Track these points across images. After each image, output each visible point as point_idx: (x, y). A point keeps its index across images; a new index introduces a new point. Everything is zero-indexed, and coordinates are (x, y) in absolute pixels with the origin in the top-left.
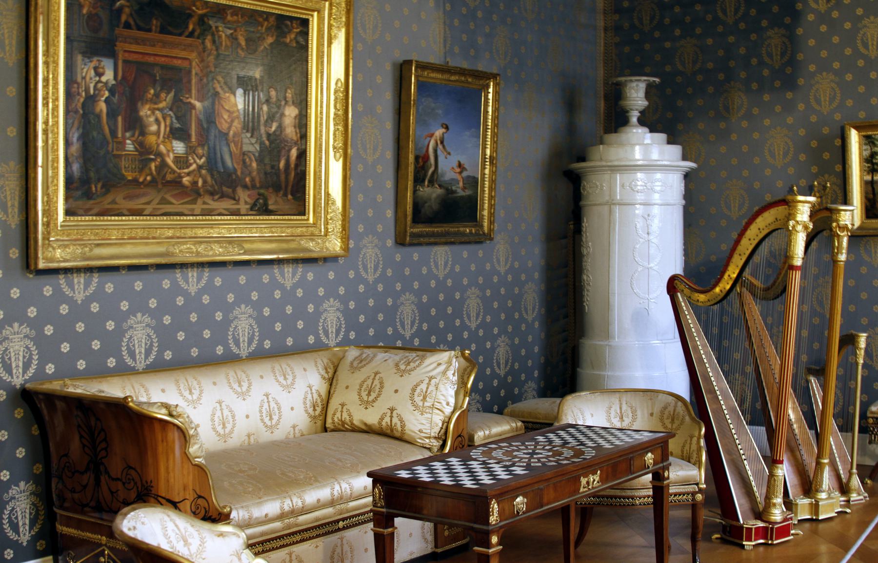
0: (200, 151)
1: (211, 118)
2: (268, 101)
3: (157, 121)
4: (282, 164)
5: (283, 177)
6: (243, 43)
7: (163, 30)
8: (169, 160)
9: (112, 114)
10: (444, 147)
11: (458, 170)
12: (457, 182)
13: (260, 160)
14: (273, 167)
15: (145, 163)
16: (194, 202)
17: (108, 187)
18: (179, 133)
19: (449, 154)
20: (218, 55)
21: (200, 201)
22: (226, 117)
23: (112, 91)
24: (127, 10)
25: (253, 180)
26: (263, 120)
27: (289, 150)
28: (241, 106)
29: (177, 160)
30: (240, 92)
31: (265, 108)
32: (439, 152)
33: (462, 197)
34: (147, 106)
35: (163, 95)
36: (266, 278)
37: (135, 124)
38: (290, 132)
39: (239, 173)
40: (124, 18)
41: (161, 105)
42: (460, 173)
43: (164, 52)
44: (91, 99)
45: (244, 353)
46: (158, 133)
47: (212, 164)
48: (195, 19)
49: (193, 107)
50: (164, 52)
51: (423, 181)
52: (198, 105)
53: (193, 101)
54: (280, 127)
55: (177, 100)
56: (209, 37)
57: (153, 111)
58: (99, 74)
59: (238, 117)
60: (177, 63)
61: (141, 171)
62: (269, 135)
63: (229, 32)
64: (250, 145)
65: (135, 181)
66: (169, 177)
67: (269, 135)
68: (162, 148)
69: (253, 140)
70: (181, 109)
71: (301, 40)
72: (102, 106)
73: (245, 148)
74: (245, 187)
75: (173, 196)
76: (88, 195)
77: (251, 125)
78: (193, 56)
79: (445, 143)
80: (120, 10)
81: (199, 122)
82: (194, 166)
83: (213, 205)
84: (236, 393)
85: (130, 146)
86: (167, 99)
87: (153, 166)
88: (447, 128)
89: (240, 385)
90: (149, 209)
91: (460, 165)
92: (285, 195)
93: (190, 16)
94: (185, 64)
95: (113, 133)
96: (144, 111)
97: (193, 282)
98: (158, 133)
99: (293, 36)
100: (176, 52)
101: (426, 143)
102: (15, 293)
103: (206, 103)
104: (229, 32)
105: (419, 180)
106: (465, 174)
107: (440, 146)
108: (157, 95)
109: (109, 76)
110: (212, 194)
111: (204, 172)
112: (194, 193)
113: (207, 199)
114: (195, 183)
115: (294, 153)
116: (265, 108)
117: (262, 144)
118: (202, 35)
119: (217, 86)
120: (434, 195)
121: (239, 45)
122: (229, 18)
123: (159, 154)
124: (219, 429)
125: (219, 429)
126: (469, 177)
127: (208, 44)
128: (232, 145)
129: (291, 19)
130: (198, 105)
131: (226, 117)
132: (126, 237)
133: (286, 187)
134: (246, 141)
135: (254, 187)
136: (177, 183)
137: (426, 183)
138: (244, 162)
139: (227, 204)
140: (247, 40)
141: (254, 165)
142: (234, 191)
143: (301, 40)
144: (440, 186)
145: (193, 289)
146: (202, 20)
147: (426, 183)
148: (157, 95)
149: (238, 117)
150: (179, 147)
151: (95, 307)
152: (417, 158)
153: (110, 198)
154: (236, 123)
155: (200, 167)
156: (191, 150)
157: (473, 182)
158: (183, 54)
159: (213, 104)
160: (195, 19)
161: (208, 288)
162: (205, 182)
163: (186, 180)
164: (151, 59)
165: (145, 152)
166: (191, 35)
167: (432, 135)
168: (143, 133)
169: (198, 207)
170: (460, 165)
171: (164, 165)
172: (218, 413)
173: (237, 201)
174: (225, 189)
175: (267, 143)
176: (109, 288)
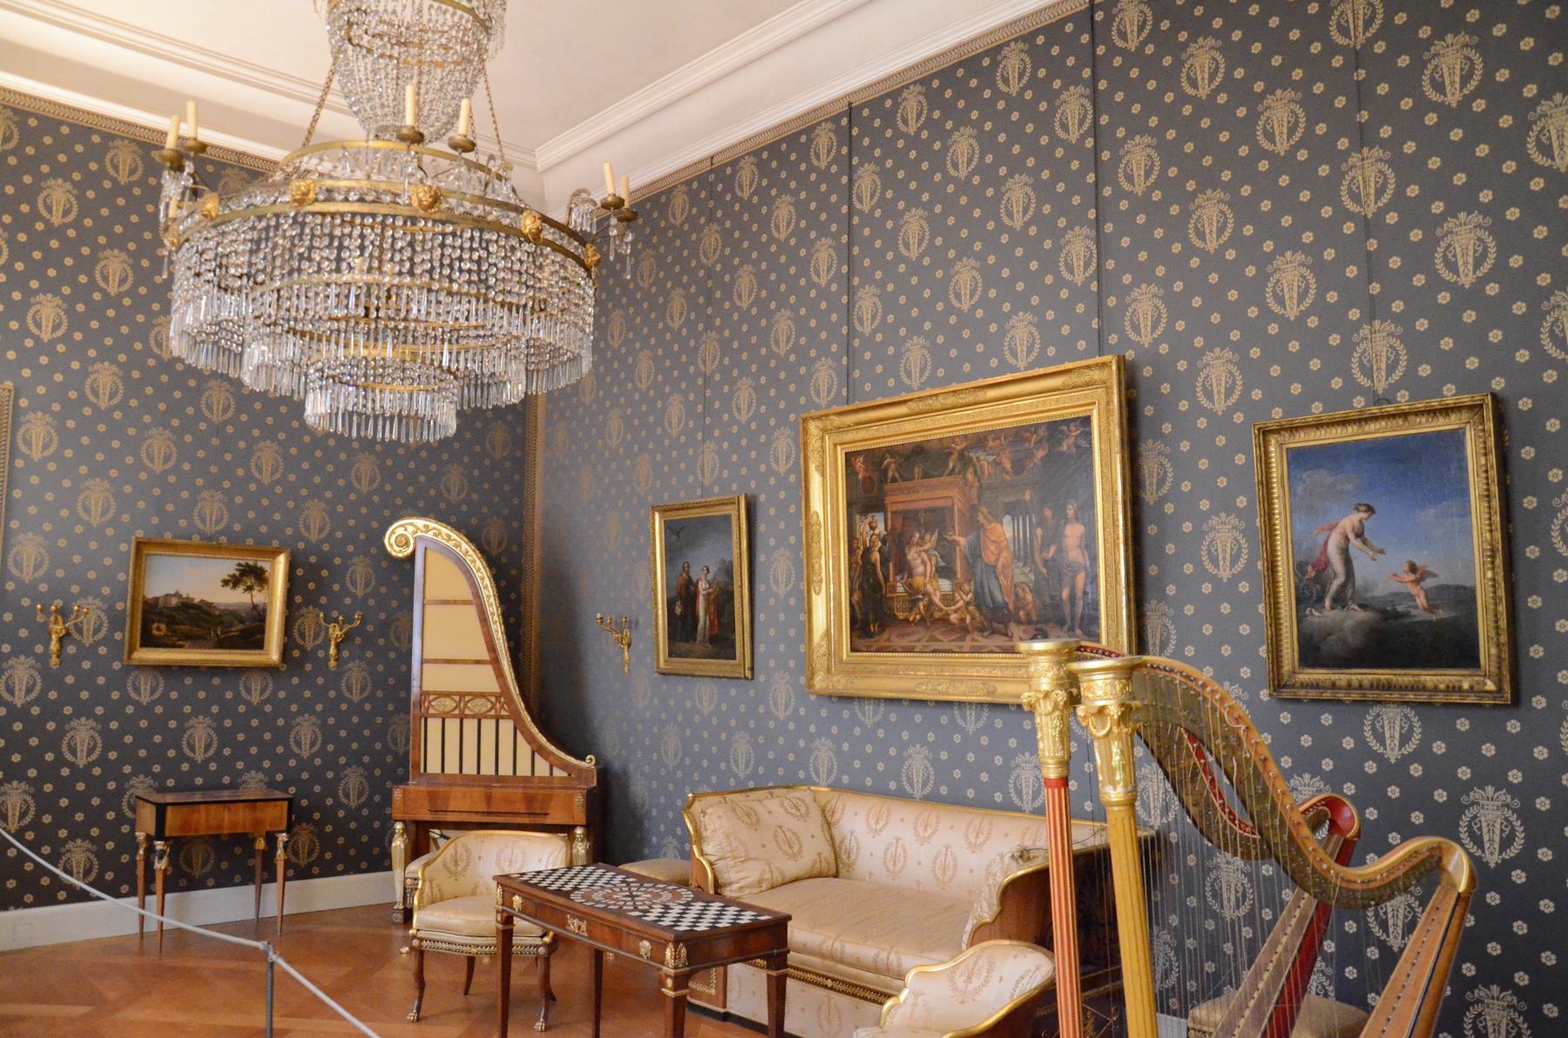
0: (966, 587)
1: (975, 553)
2: (1041, 522)
3: (923, 562)
4: (1065, 594)
5: (1067, 610)
6: (1008, 466)
7: (926, 475)
8: (937, 599)
9: (884, 562)
10: (1365, 542)
11: (1412, 577)
12: (1411, 597)
13: (1036, 591)
14: (1052, 598)
15: (914, 602)
16: (962, 639)
17: (883, 628)
18: (945, 571)
19: (1382, 552)
20: (981, 487)
21: (969, 638)
22: (992, 548)
23: (884, 541)
24: (893, 466)
25: (1028, 615)
26: (1037, 545)
27: (1074, 577)
28: (1009, 535)
29: (944, 598)
30: (1007, 519)
31: (1039, 532)
32: (1353, 552)
33: (1423, 623)
34: (913, 550)
35: (927, 537)
36: (944, 719)
37: (904, 568)
38: (1075, 554)
39: (1011, 607)
40: (890, 474)
41: (928, 546)
42: (1417, 582)
43: (927, 495)
44: (868, 551)
45: (918, 794)
46: (924, 574)
47: (978, 601)
48: (954, 457)
49: (958, 543)
50: (927, 495)
51: (1321, 599)
52: (962, 540)
53: (956, 537)
54: (1060, 550)
55: (941, 538)
56: (971, 470)
57: (919, 553)
58: (873, 528)
59: (1007, 547)
60: (940, 503)
61: (911, 610)
62: (1046, 562)
63: (991, 458)
64: (1023, 575)
65: (906, 620)
66: (937, 615)
67: (1046, 562)
68: (929, 588)
69: (1027, 570)
70: (946, 548)
71: (1083, 443)
72: (876, 556)
73: (1020, 578)
74: (1019, 622)
75: (943, 633)
76: (867, 634)
77: (1024, 554)
78: (954, 493)
79: (1366, 535)
80: (886, 470)
81: (965, 557)
82: (961, 603)
83: (983, 642)
84: (970, 843)
85: (900, 589)
86: (931, 540)
87: (921, 605)
88: (1370, 509)
89: (977, 836)
90: (919, 646)
91: (1413, 568)
92: (1072, 629)
93: (950, 454)
94: (949, 503)
95: (886, 578)
96: (912, 555)
97: (869, 715)
98: (924, 574)
99: (1071, 441)
100: (940, 493)
101: (1321, 540)
102: (824, 713)
103: (971, 537)
104: (991, 458)
105: (1305, 599)
106: (1429, 583)
107: (1355, 543)
108: (922, 538)
109: (881, 529)
110: (981, 630)
111: (971, 608)
112: (962, 630)
113: (976, 635)
114: (963, 620)
115: (1081, 579)
116: (1039, 532)
117: (1037, 573)
118: (963, 471)
119: (981, 517)
120: (1349, 623)
121: (1004, 469)
122: (991, 443)
123: (926, 594)
124: (939, 873)
125: (939, 873)
126: (1442, 589)
127: (970, 476)
128: (1002, 578)
129: (1067, 422)
130: (962, 540)
131: (992, 548)
132: (909, 672)
133: (1073, 619)
134: (1017, 571)
135: (1030, 622)
136: (945, 620)
137: (1328, 603)
138: (1017, 595)
139: (1000, 641)
140: (1013, 463)
141: (1029, 597)
142: (1006, 627)
143: (1083, 443)
144: (1363, 606)
145: (971, 728)
146: (962, 455)
147: (1328, 603)
148: (922, 538)
149: (1007, 547)
150: (945, 585)
151: (984, 741)
152: (1300, 568)
153: (885, 636)
154: (1004, 554)
155: (968, 603)
156: (957, 587)
157: (1464, 597)
158: (946, 493)
159: (978, 538)
160: (954, 457)
161: (988, 729)
162: (973, 619)
163: (953, 618)
164: (911, 506)
165: (914, 595)
166: (952, 473)
167: (1332, 528)
168: (911, 575)
169: (968, 644)
170: (1413, 568)
171: (931, 603)
172: (942, 857)
173: (1011, 638)
174: (995, 625)
175: (1044, 571)
176: (893, 717)
